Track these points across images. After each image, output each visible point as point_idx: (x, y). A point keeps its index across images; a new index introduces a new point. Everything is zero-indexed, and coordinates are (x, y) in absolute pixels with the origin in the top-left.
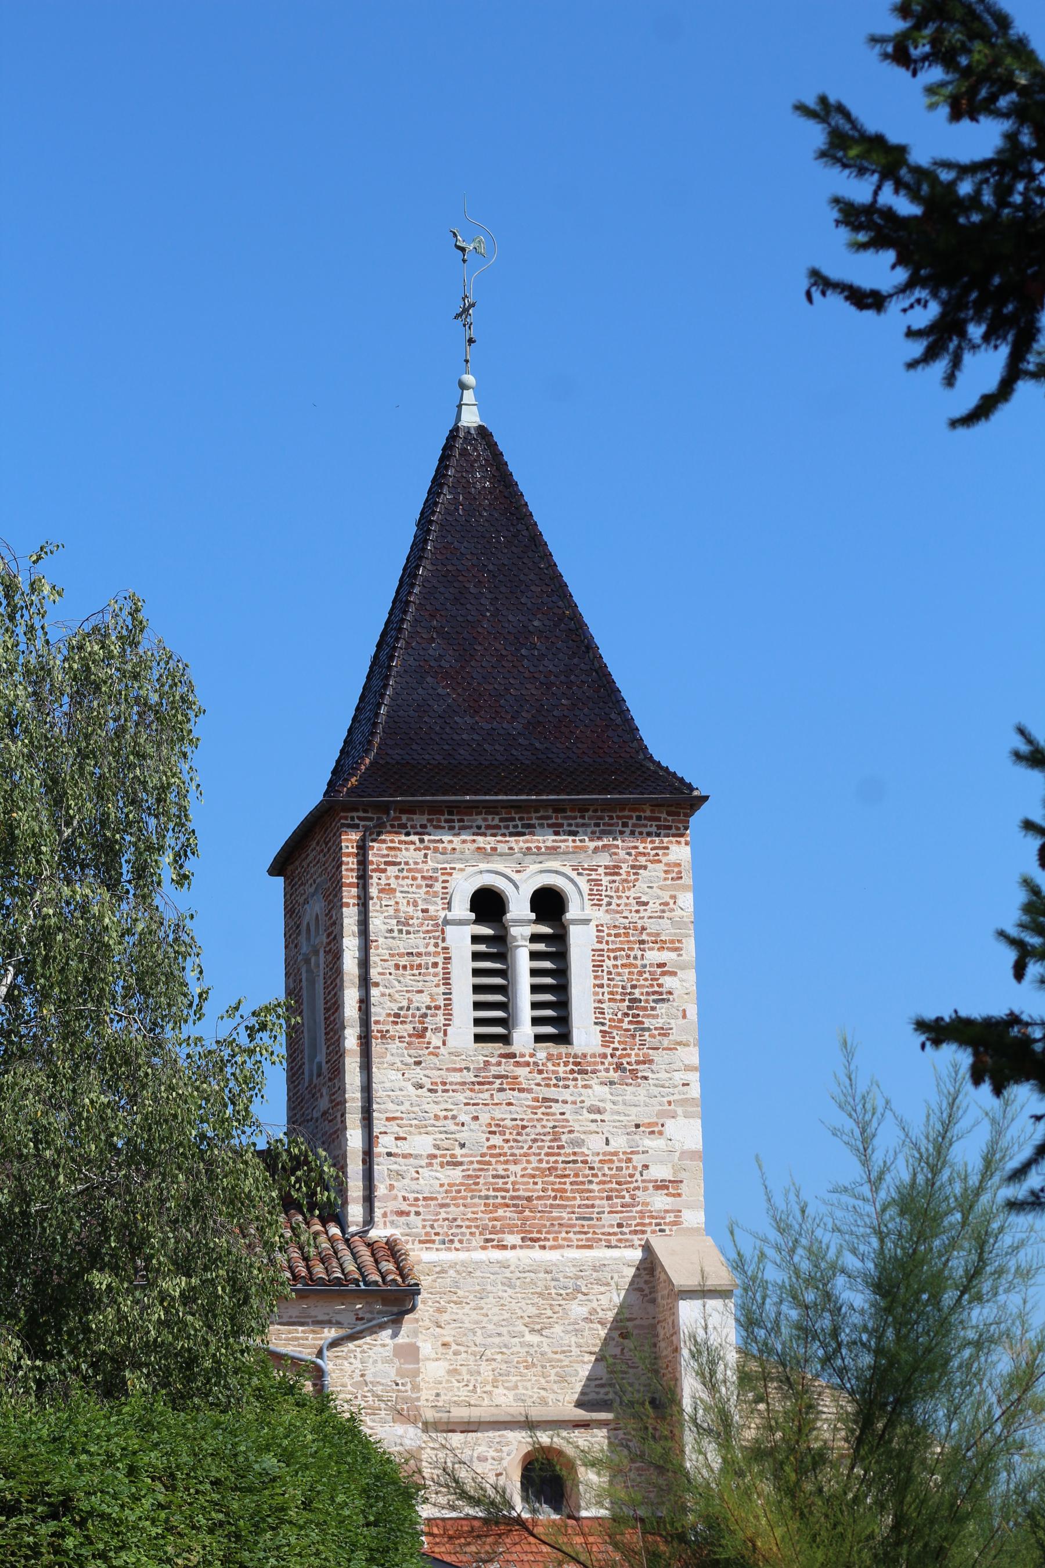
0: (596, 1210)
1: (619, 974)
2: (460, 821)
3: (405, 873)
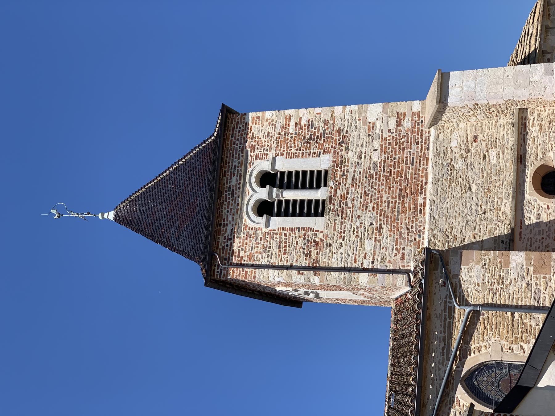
0: (409, 156)
1: (298, 146)
2: (224, 221)
3: (244, 248)
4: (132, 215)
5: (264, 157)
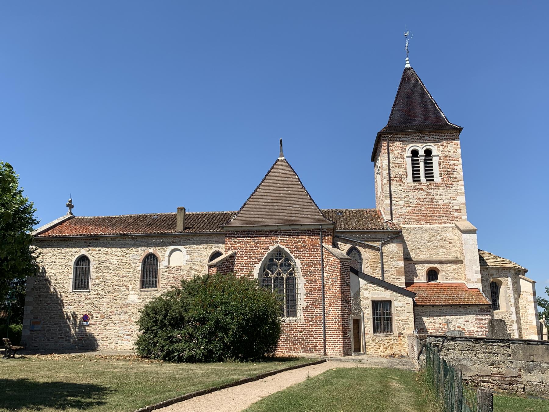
4: (409, 79)
5: (439, 151)
